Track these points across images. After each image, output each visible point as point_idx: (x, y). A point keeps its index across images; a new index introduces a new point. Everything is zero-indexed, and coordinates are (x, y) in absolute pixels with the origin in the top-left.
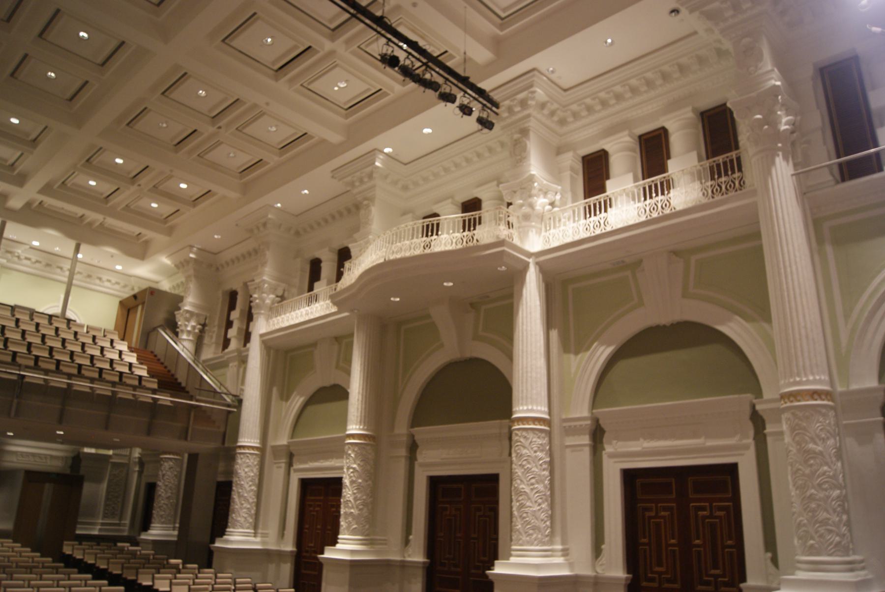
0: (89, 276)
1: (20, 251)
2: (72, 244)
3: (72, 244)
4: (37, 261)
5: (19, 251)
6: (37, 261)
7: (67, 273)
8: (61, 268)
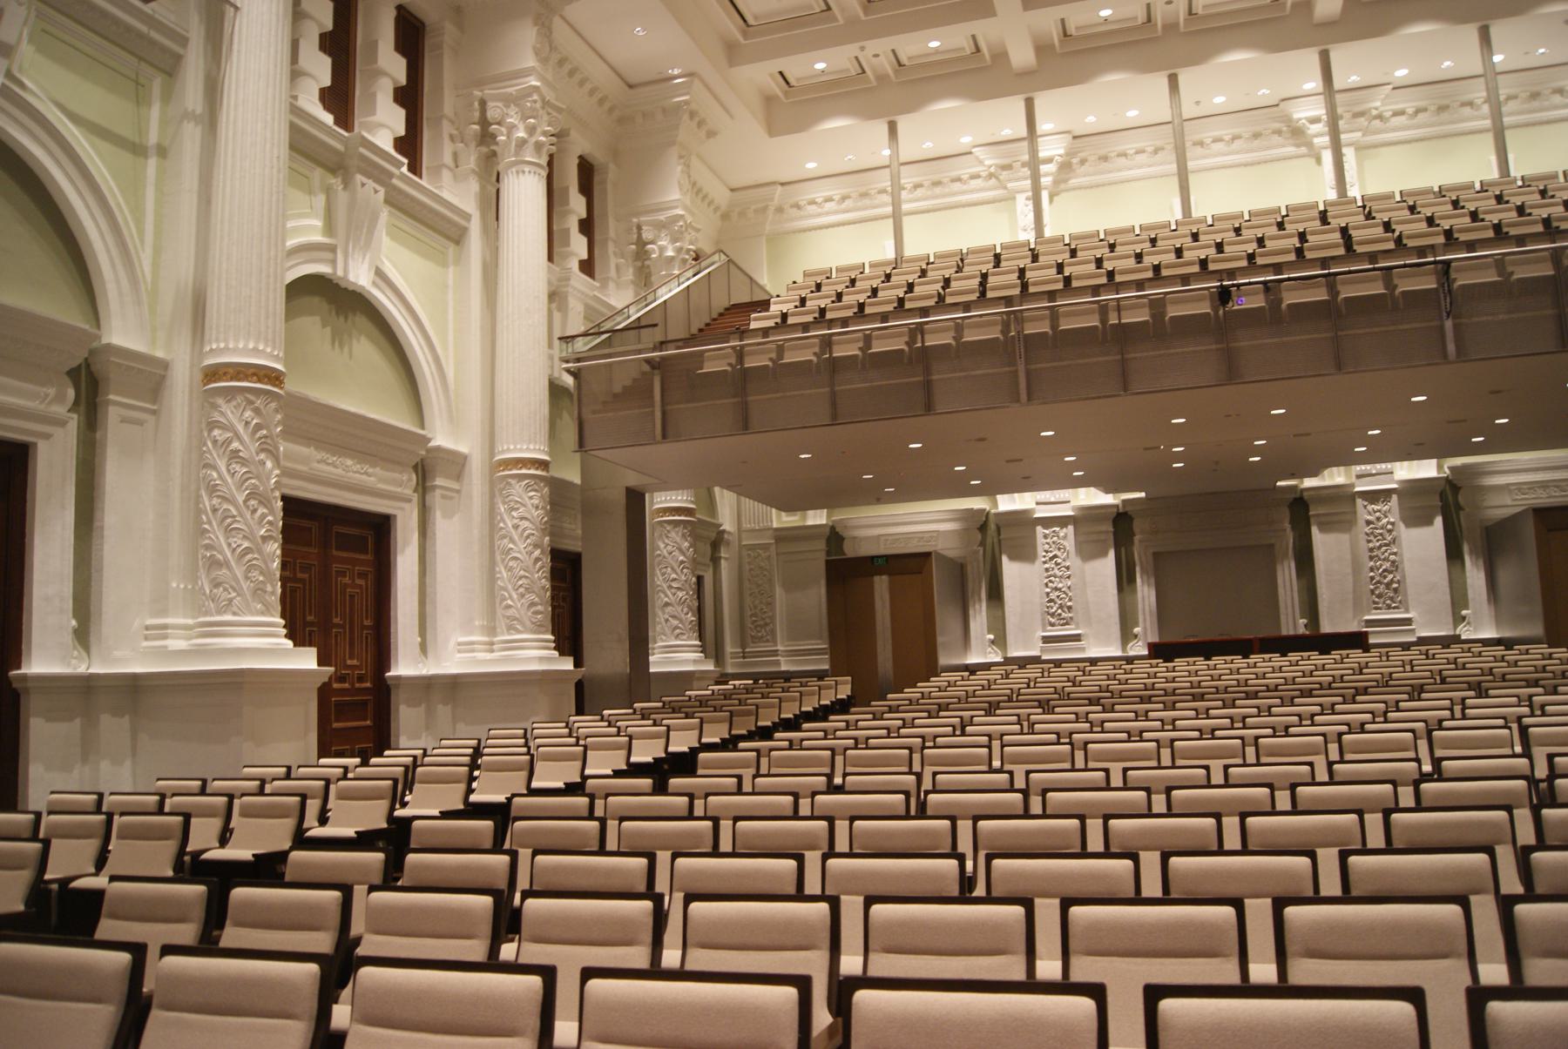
0: (1535, 96)
1: (1378, 104)
2: (1470, 33)
3: (1470, 33)
4: (1417, 111)
5: (1377, 103)
6: (1417, 111)
7: (1486, 109)
8: (1470, 104)
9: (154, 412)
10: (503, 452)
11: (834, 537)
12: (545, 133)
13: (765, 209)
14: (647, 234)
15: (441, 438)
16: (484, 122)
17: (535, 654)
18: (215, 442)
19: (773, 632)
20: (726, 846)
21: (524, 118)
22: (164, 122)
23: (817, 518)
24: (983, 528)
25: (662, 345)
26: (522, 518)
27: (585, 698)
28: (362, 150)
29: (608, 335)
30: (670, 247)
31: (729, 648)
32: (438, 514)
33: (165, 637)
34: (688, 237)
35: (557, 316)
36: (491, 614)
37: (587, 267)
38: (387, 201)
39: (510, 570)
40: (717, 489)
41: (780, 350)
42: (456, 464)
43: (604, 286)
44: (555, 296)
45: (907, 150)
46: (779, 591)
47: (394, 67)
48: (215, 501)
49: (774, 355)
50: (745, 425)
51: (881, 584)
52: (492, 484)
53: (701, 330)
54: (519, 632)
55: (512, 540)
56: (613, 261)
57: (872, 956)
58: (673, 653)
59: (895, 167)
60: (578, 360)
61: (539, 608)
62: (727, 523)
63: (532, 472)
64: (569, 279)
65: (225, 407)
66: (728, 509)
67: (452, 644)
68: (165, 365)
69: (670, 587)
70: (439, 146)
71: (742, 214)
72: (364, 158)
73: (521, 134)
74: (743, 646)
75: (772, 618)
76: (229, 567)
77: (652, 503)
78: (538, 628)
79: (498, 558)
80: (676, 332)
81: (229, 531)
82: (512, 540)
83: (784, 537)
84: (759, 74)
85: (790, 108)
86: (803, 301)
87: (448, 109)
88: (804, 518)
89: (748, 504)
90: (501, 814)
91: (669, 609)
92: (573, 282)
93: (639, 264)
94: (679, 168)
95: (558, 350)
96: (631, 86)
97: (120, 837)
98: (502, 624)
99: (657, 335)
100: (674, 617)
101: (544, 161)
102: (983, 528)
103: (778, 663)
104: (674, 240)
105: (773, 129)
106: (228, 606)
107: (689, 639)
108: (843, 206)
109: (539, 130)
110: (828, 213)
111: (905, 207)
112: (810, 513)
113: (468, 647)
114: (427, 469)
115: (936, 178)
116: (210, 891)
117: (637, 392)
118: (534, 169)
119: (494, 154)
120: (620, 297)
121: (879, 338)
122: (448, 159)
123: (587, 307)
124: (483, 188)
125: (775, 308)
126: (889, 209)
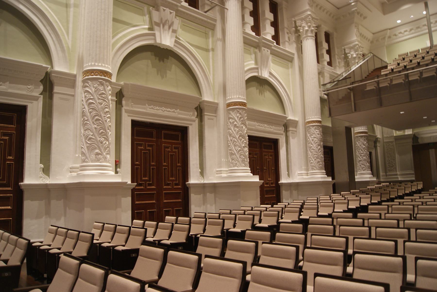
9: (216, 116)
10: (308, 119)
12: (313, 27)
14: (347, 51)
15: (290, 117)
16: (296, 27)
17: (320, 176)
18: (230, 123)
19: (396, 168)
20: (373, 236)
21: (307, 23)
22: (213, 42)
23: (409, 132)
25: (353, 83)
26: (314, 138)
27: (335, 189)
28: (263, 41)
29: (337, 82)
30: (355, 54)
31: (381, 173)
32: (291, 138)
33: (221, 173)
34: (360, 50)
35: (321, 79)
36: (307, 165)
37: (330, 64)
38: (271, 53)
39: (312, 152)
40: (375, 125)
41: (391, 80)
42: (295, 123)
43: (335, 68)
44: (320, 73)
45: (431, 11)
46: (397, 156)
47: (270, 16)
48: (231, 138)
49: (389, 82)
50: (381, 104)
51: (432, 152)
52: (305, 128)
53: (366, 77)
54: (315, 170)
55: (312, 144)
56: (337, 61)
57: (418, 277)
58: (363, 175)
59: (428, 17)
60: (328, 91)
61: (321, 163)
62: (379, 135)
63: (317, 124)
64: (324, 68)
65: (232, 113)
66: (379, 131)
67: (296, 174)
68: (217, 104)
69: (361, 156)
70: (284, 36)
71: (377, 40)
72: (264, 43)
73: (307, 28)
74: (386, 172)
75: (395, 164)
76: (236, 155)
77: (354, 131)
78: (320, 169)
79: (308, 149)
80: (358, 78)
81: (235, 146)
82: (312, 144)
83: (397, 138)
86: (399, 64)
87: (286, 25)
88: (404, 132)
89: (385, 129)
90: (305, 222)
91: (361, 162)
92: (325, 68)
93: (345, 60)
94: (355, 30)
95: (322, 88)
96: (338, 9)
97: (208, 224)
98: (310, 167)
99: (352, 80)
100: (363, 164)
101: (314, 35)
103: (398, 178)
104: (355, 52)
105: (385, 13)
106: (236, 165)
107: (368, 171)
108: (411, 32)
109: (312, 26)
110: (406, 36)
111: (433, 29)
112: (406, 130)
113: (301, 174)
114: (287, 126)
116: (223, 241)
117: (346, 98)
118: (311, 38)
119: (300, 35)
120: (340, 71)
121: (425, 72)
122: (287, 39)
123: (330, 75)
124: (297, 46)
125: (389, 68)
126: (427, 31)
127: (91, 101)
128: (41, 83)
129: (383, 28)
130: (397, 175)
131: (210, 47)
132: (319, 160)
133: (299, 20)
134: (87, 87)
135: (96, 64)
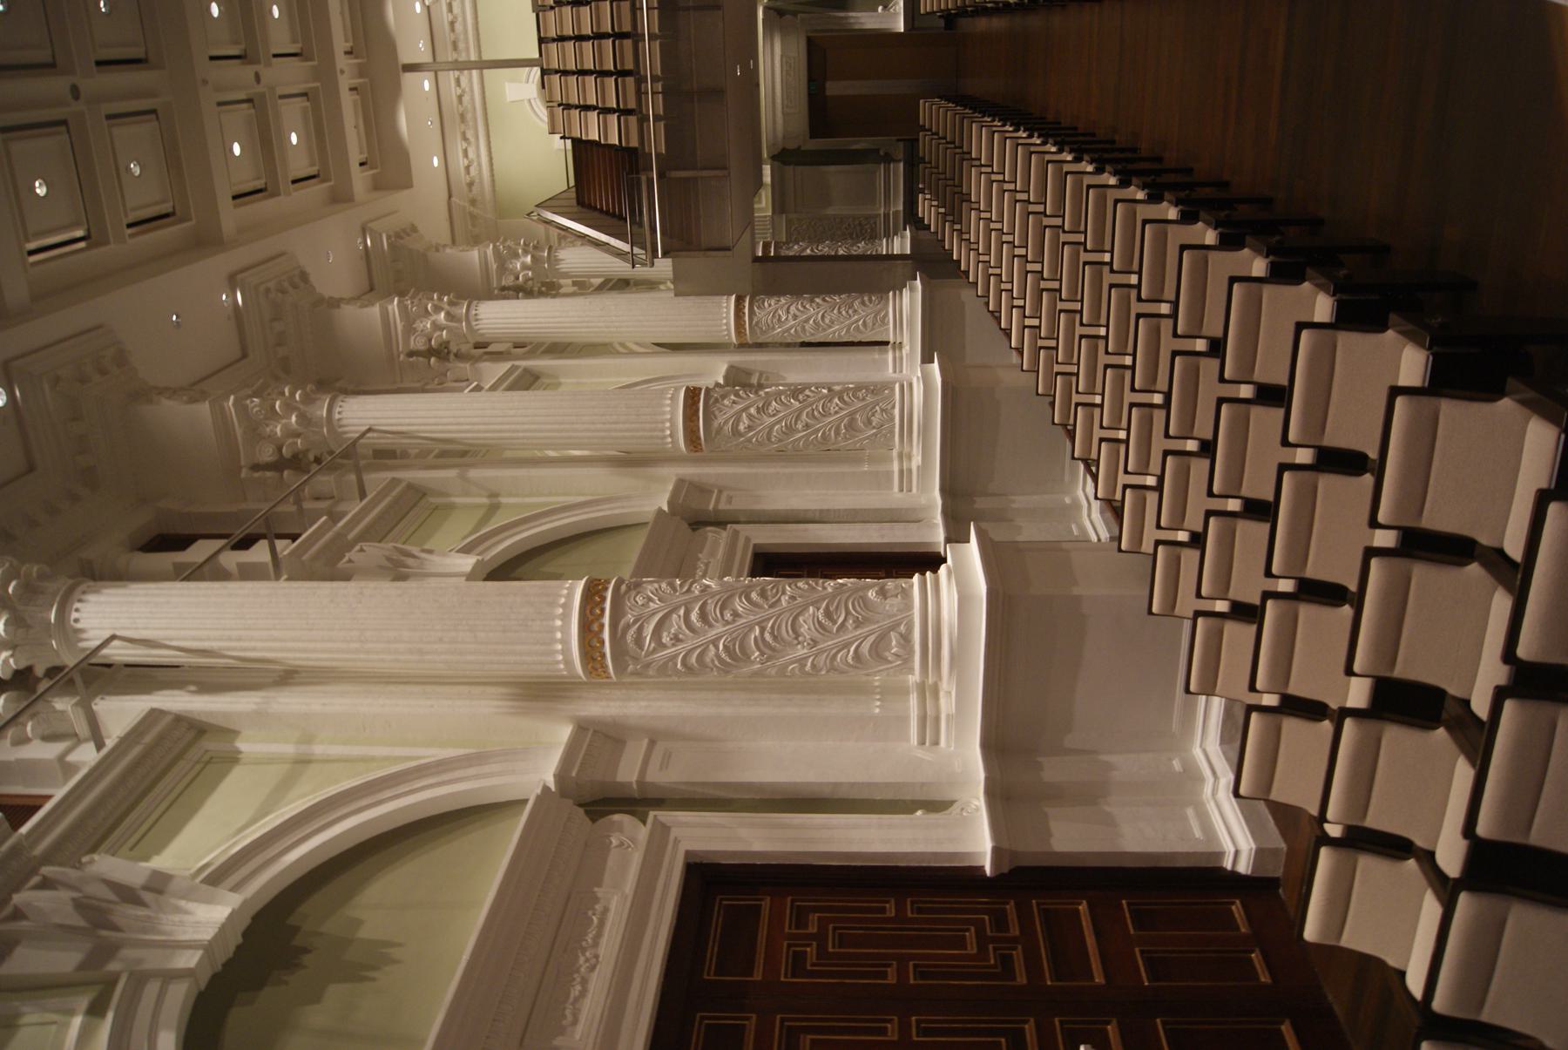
9: (720, 492)
11: (783, 157)
13: (473, 217)
18: (750, 428)
19: (868, 218)
22: (467, 494)
24: (780, 13)
33: (910, 471)
39: (832, 322)
46: (830, 211)
48: (800, 426)
51: (834, 88)
54: (887, 315)
55: (807, 321)
65: (721, 420)
68: (680, 482)
76: (855, 412)
81: (826, 414)
82: (807, 321)
83: (780, 206)
84: (360, 180)
85: (390, 164)
102: (780, 13)
103: (896, 213)
104: (516, 256)
105: (408, 185)
106: (888, 412)
110: (478, 156)
115: (450, 47)
127: (694, 616)
128: (602, 821)
129: (445, 214)
130: (887, 216)
131: (485, 500)
132: (856, 304)
133: (407, 341)
134: (640, 629)
135: (563, 600)
